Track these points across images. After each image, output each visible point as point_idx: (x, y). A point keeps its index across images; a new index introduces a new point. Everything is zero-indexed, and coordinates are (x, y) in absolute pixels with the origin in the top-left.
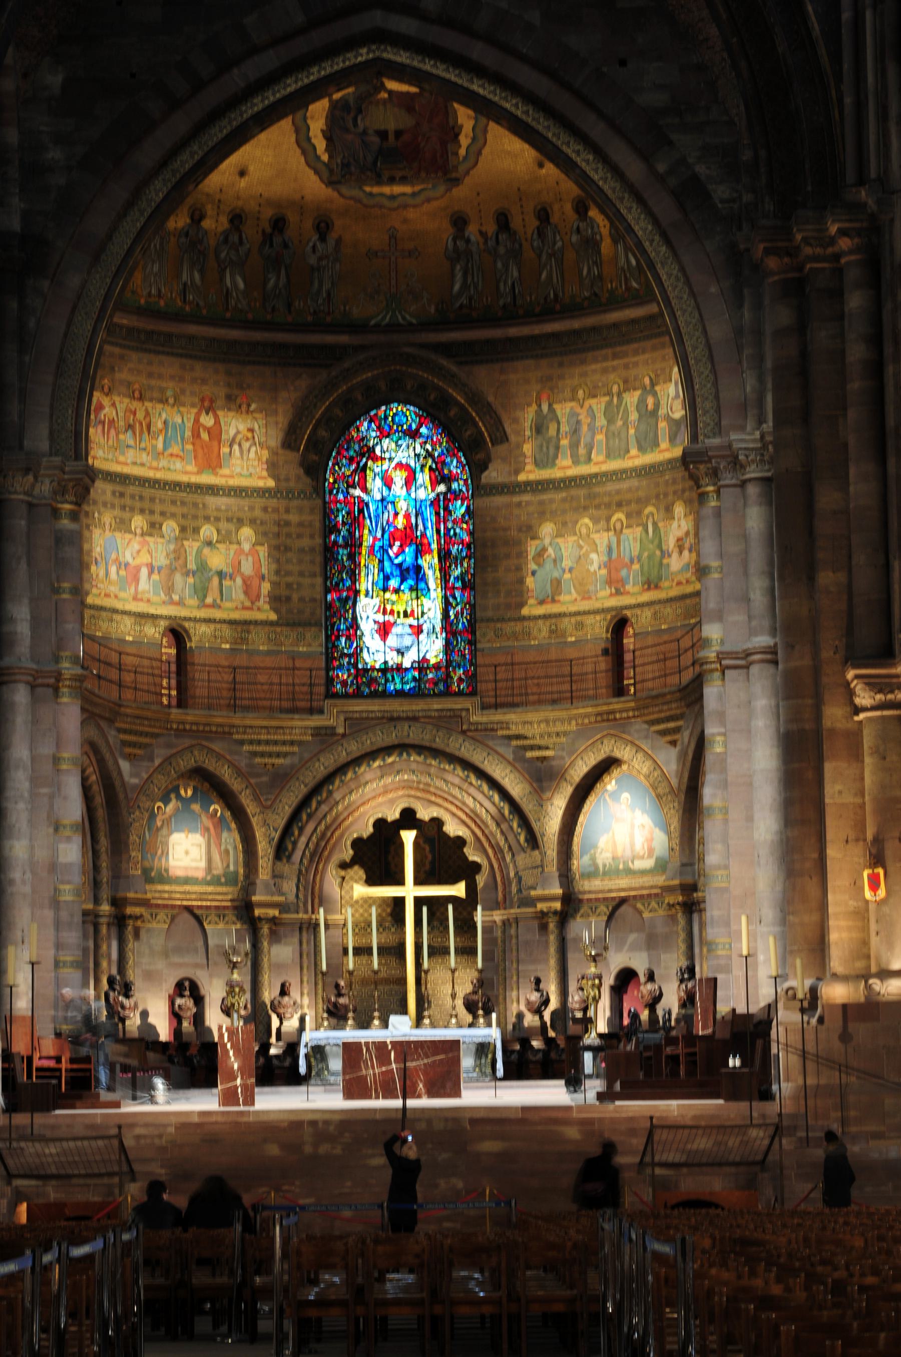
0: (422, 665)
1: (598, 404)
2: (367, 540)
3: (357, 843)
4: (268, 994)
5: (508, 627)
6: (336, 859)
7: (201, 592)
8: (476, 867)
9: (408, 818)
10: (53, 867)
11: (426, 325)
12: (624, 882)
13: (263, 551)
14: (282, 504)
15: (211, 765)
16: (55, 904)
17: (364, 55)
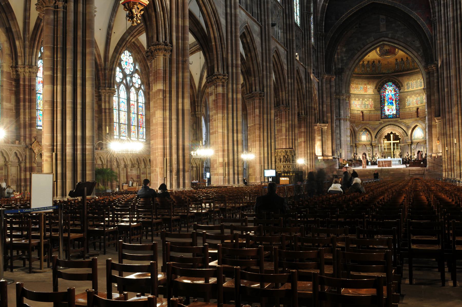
0: (393, 114)
1: (415, 81)
2: (386, 99)
3: (385, 136)
4: (374, 154)
5: (404, 109)
6: (382, 138)
7: (365, 107)
8: (400, 139)
9: (392, 133)
10: (347, 141)
11: (393, 73)
12: (419, 140)
13: (373, 102)
14: (375, 96)
15: (367, 128)
16: (347, 145)
17: (382, 43)
